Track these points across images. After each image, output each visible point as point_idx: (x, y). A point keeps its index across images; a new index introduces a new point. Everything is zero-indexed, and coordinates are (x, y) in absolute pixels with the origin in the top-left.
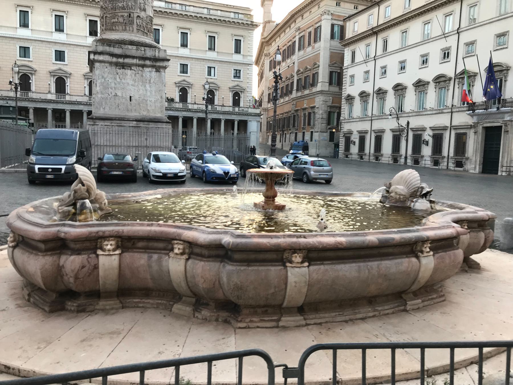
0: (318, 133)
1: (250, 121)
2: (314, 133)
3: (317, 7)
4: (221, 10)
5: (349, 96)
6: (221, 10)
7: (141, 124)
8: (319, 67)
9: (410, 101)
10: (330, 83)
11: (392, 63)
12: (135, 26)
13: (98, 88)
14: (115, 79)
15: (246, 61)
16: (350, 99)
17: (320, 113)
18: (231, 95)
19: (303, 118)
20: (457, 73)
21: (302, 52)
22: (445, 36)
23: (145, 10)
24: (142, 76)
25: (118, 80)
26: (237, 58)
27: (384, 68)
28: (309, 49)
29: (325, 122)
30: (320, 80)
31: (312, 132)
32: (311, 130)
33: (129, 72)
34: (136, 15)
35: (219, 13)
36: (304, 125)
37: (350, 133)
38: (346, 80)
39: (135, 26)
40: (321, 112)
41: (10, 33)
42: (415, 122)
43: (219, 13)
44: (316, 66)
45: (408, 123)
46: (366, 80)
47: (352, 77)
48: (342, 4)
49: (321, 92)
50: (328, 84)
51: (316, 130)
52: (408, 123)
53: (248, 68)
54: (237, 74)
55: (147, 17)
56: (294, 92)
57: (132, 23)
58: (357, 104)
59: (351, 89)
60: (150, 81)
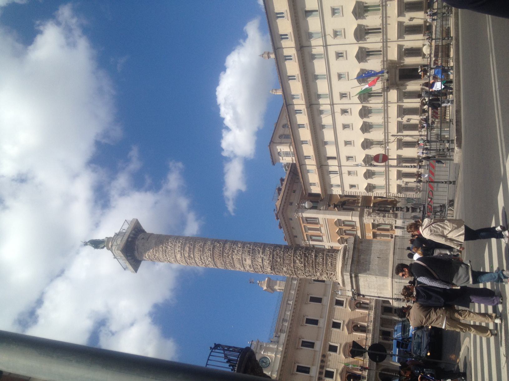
0: (397, 220)
2: (397, 225)
5: (366, 189)
8: (338, 220)
9: (376, 135)
10: (353, 210)
11: (345, 151)
16: (370, 188)
19: (382, 238)
20: (359, 102)
21: (325, 238)
22: (333, 114)
29: (387, 215)
30: (349, 218)
31: (396, 227)
32: (394, 228)
33: (362, 257)
36: (387, 236)
37: (399, 187)
38: (353, 192)
40: (377, 217)
42: (393, 128)
44: (338, 223)
45: (393, 136)
46: (356, 173)
48: (291, 201)
49: (361, 216)
50: (354, 212)
51: (394, 222)
52: (393, 136)
58: (375, 181)
59: (361, 190)
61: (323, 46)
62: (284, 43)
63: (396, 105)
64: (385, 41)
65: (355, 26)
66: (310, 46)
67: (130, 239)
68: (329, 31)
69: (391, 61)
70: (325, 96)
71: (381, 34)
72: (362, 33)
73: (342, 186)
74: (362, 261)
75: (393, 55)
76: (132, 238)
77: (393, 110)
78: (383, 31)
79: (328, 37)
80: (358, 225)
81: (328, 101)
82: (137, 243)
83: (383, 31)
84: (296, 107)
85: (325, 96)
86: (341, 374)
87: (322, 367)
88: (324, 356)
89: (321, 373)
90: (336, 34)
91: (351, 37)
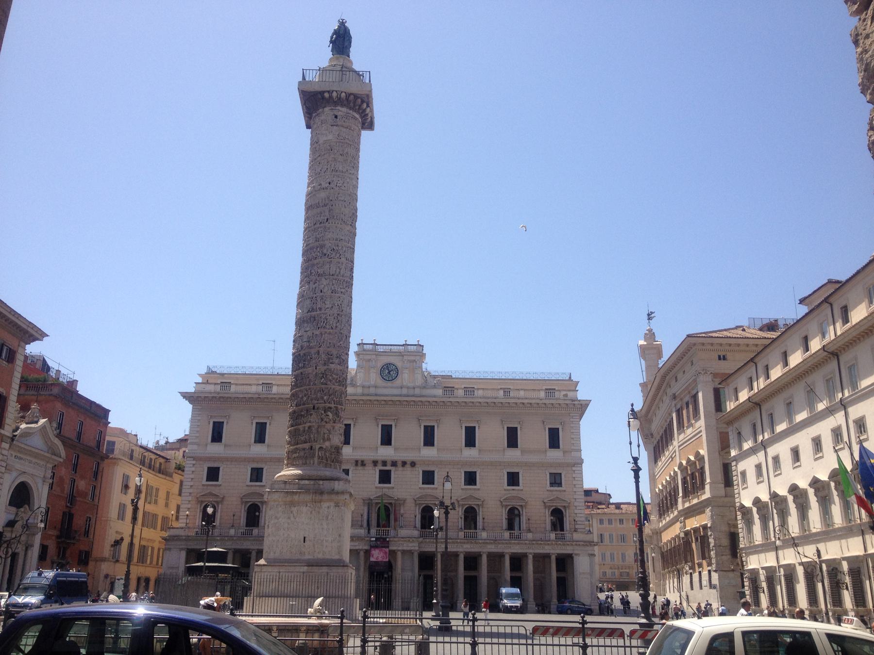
1: (576, 554)
3: (690, 364)
4: (525, 390)
6: (525, 390)
7: (315, 569)
12: (316, 459)
13: (270, 530)
14: (289, 518)
23: (329, 439)
24: (319, 512)
25: (292, 519)
26: (554, 455)
28: (689, 431)
30: (708, 480)
34: (318, 447)
35: (522, 393)
39: (316, 459)
41: (242, 453)
43: (522, 393)
45: (818, 551)
47: (744, 474)
50: (723, 485)
53: (574, 468)
54: (556, 480)
55: (331, 447)
56: (680, 500)
57: (313, 456)
60: (327, 517)
67: (327, 95)
74: (295, 509)
76: (339, 98)
82: (327, 109)
87: (394, 464)
88: (413, 464)
89: (384, 463)
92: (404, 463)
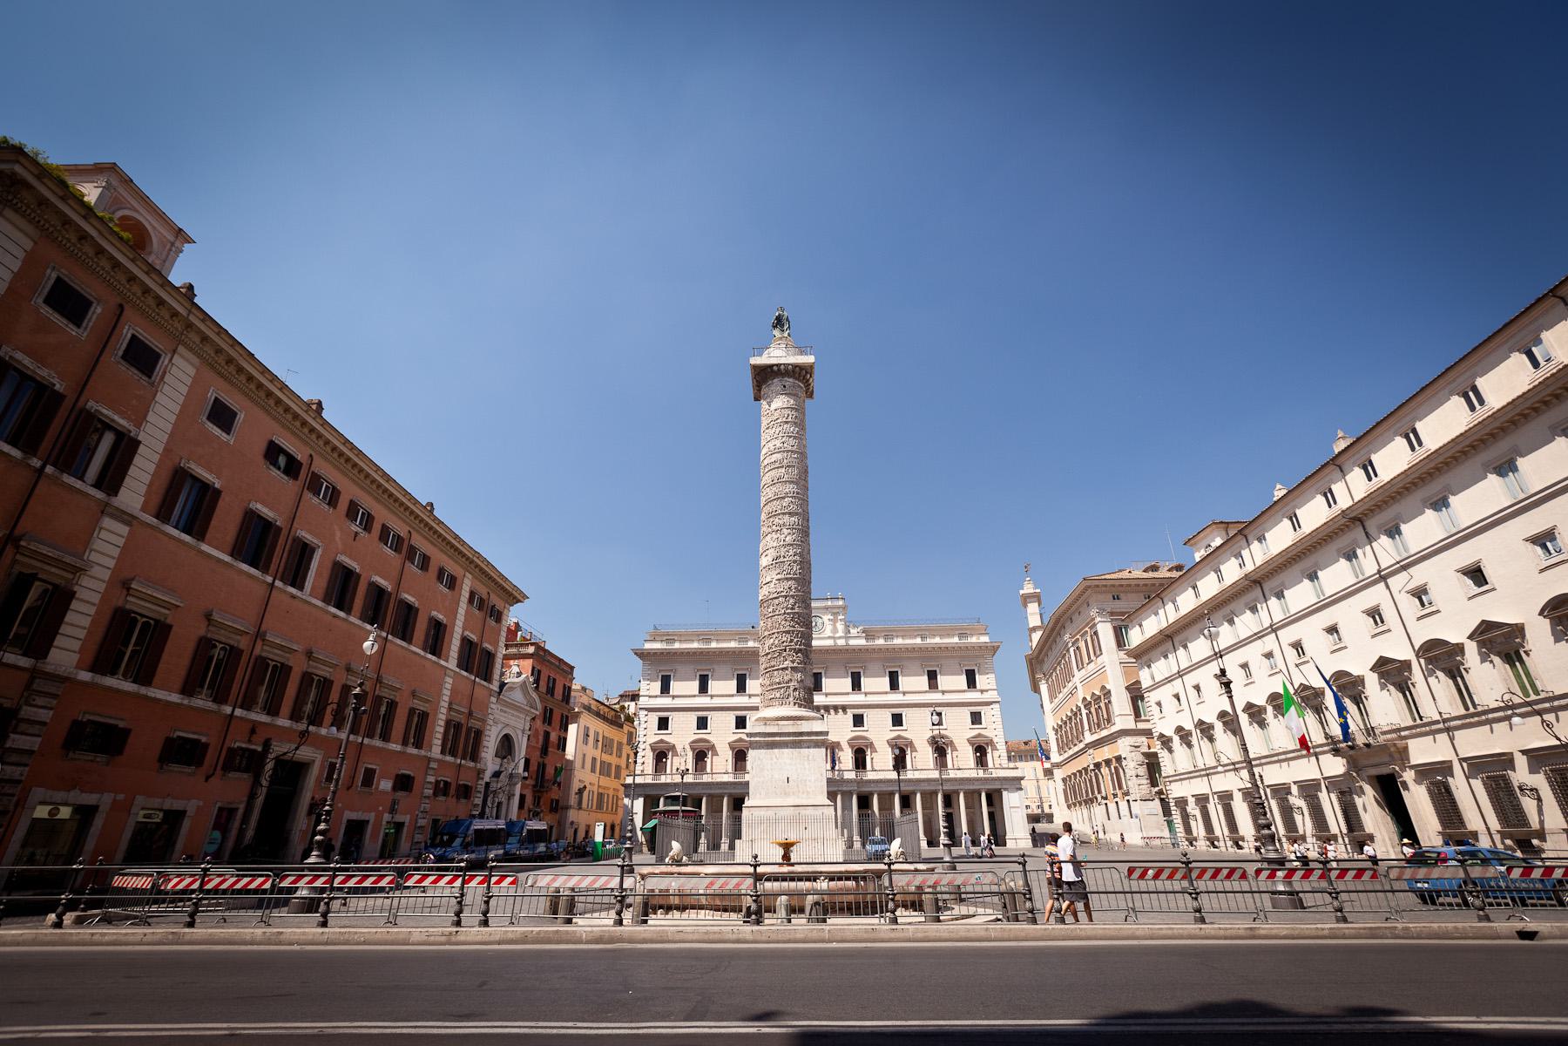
15: (987, 697)
17: (1133, 766)
18: (970, 750)
27: (1197, 688)
43: (937, 640)
61: (1379, 572)
62: (1356, 476)
63: (1319, 776)
64: (1447, 727)
65: (1453, 638)
66: (1370, 539)
68: (1419, 575)
69: (1406, 748)
70: (1285, 609)
71: (1463, 712)
72: (1442, 657)
73: (1156, 686)
75: (1423, 751)
77: (1305, 770)
78: (1472, 715)
79: (1404, 575)
80: (1114, 729)
81: (1278, 617)
83: (1472, 715)
84: (1245, 553)
85: (1285, 609)
86: (979, 735)
88: (844, 708)
90: (1419, 593)
91: (1425, 632)
92: (836, 708)
